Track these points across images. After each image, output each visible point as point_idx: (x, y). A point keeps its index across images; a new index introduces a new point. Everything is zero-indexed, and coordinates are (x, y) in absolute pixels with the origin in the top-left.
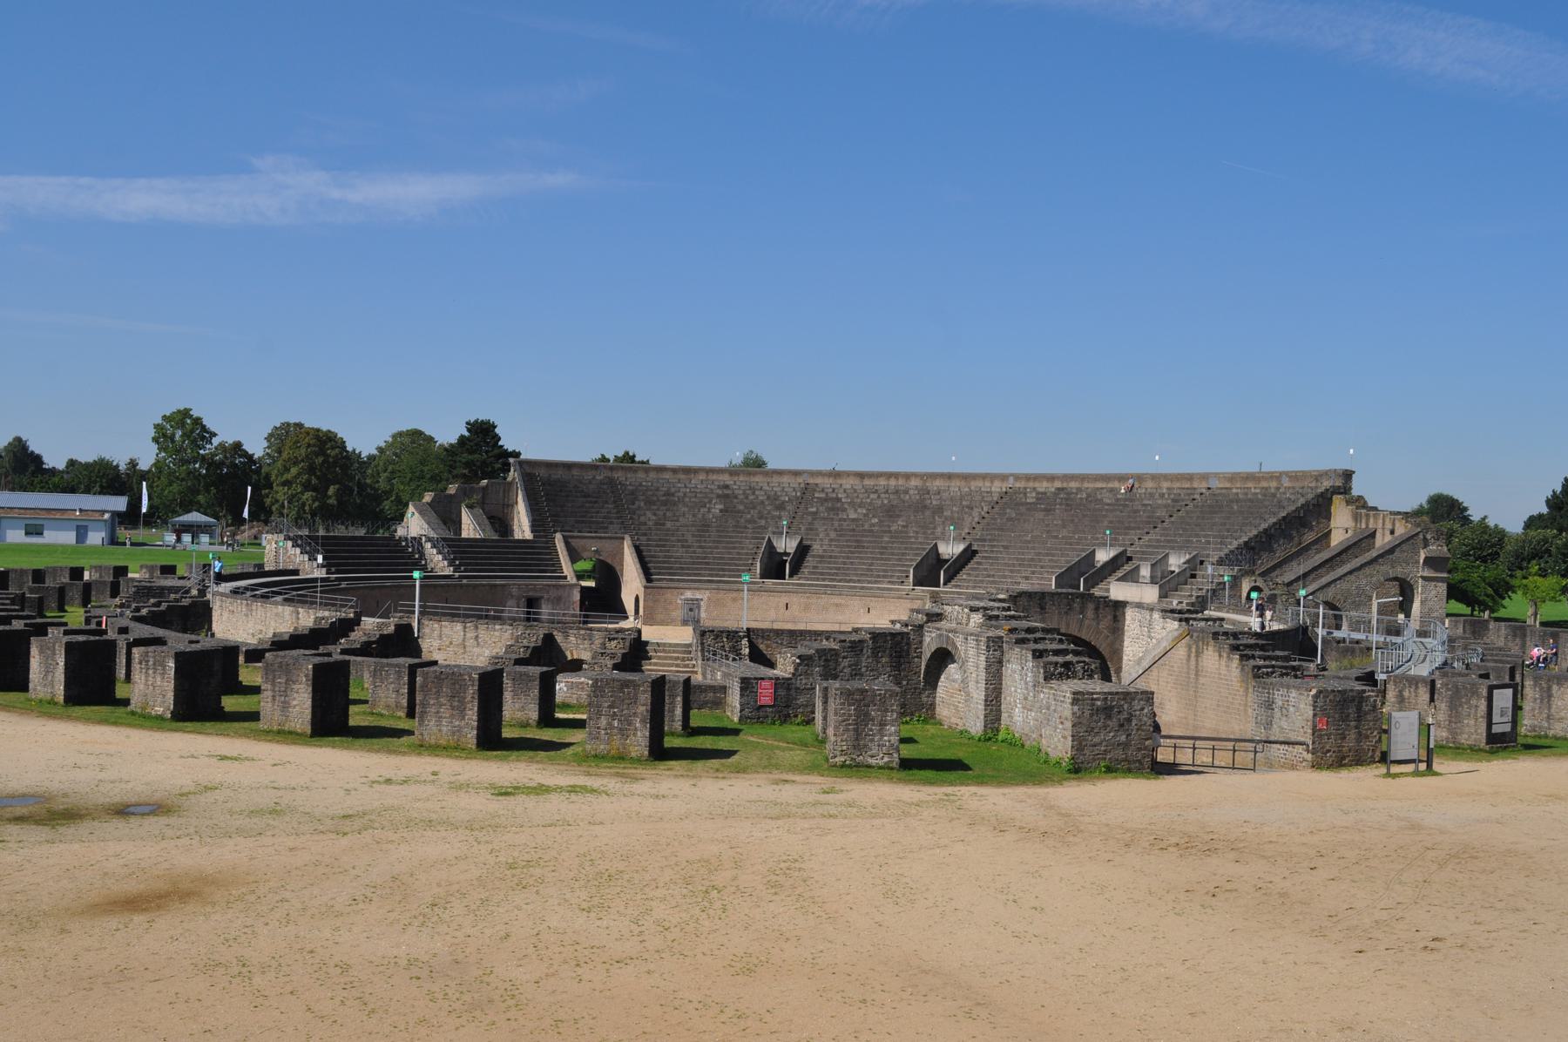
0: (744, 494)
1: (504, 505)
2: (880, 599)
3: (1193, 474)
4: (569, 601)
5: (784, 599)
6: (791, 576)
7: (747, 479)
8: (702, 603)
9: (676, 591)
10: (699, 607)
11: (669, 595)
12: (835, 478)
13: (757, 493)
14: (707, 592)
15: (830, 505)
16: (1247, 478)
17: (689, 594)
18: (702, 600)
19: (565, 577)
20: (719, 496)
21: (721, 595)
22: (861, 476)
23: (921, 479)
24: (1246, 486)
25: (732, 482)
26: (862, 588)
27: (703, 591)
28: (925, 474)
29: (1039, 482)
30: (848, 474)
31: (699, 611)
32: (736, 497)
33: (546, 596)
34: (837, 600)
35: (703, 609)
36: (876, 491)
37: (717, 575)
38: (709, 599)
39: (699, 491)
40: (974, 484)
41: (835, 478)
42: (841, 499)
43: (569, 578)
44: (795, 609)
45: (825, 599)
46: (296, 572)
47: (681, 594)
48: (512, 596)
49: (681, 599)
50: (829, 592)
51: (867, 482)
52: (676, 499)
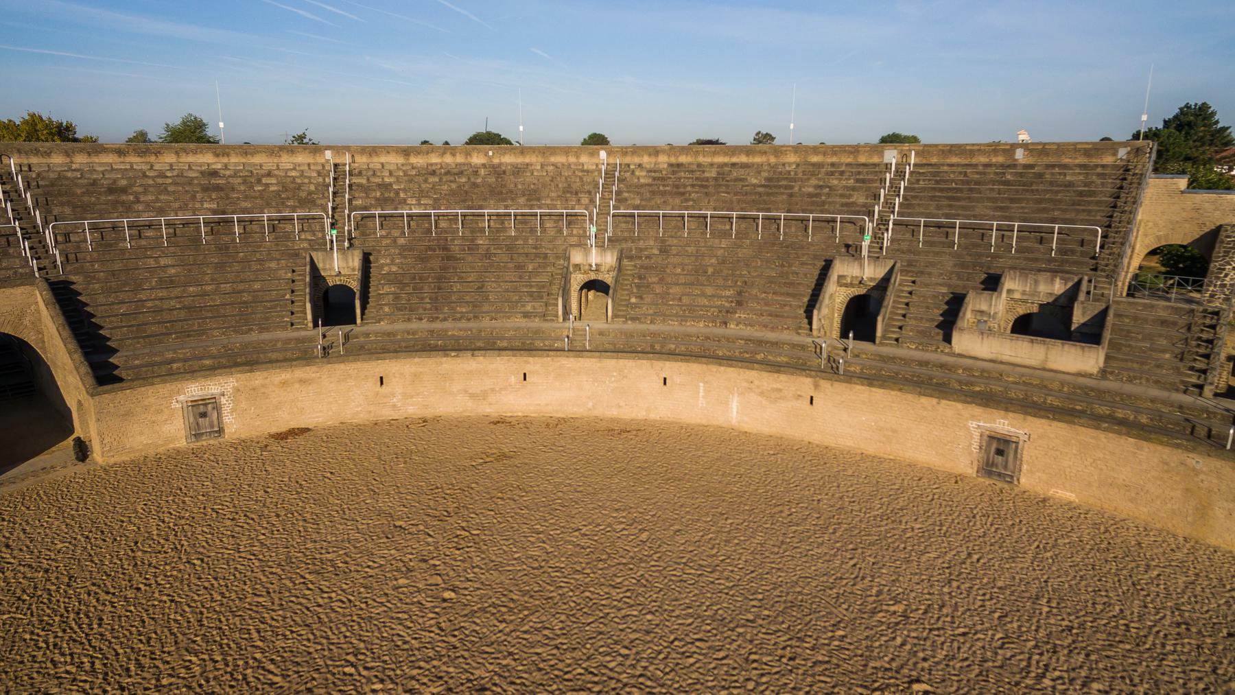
0: (245, 182)
3: (858, 146)
7: (244, 160)
8: (223, 400)
10: (218, 408)
13: (264, 180)
15: (378, 194)
16: (950, 151)
20: (205, 189)
24: (871, 161)
25: (219, 166)
30: (388, 150)
32: (233, 189)
35: (226, 411)
36: (433, 173)
39: (170, 181)
40: (560, 159)
42: (390, 184)
44: (395, 387)
47: (178, 393)
52: (131, 198)
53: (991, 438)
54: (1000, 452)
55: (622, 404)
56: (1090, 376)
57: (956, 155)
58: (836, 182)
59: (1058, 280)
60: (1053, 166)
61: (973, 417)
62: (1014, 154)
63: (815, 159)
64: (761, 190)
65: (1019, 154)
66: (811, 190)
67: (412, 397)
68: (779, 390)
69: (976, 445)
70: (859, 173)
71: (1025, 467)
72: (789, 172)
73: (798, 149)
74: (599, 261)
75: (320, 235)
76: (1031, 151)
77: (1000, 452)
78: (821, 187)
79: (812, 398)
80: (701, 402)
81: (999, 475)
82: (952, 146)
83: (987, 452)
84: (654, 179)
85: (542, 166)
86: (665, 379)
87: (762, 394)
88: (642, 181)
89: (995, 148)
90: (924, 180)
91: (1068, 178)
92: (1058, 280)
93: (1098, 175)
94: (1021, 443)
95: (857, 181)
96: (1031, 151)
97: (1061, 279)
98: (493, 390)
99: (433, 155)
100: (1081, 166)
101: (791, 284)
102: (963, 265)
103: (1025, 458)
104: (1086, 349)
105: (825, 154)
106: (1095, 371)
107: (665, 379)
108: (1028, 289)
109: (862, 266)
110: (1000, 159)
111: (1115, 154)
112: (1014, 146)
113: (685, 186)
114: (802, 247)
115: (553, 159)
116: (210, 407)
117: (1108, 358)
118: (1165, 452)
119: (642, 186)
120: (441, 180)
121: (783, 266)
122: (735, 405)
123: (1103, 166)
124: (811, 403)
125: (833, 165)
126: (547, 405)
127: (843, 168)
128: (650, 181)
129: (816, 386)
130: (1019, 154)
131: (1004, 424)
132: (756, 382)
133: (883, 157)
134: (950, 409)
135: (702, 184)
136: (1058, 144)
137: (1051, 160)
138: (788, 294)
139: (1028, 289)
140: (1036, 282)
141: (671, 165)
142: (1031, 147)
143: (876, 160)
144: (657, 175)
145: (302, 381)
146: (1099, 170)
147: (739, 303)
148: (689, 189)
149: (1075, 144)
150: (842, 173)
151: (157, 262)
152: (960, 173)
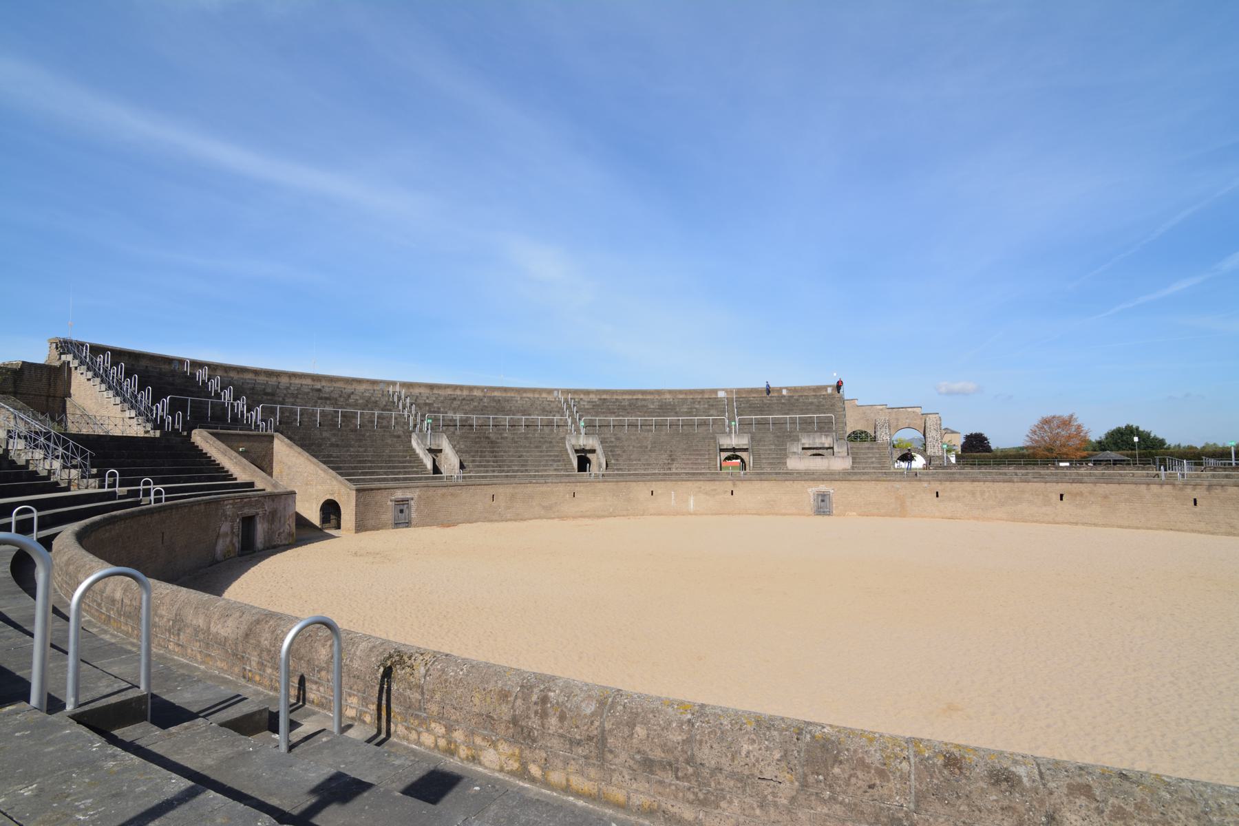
1: (48, 396)
2: (585, 484)
4: (285, 516)
5: (490, 490)
6: (442, 473)
8: (412, 503)
9: (385, 493)
10: (409, 508)
11: (379, 496)
12: (409, 388)
14: (418, 490)
17: (399, 495)
18: (412, 499)
19: (251, 485)
21: (430, 492)
22: (431, 387)
23: (482, 391)
26: (507, 476)
27: (413, 490)
28: (486, 388)
29: (577, 394)
31: (410, 512)
33: (260, 512)
34: (544, 488)
35: (413, 509)
37: (393, 473)
38: (419, 497)
41: (409, 388)
43: (259, 485)
45: (530, 489)
46: (264, 490)
48: (226, 516)
49: (391, 501)
50: (534, 481)
51: (435, 391)
53: (818, 495)
54: (823, 501)
55: (629, 508)
58: (697, 406)
59: (823, 436)
60: (802, 396)
61: (809, 487)
63: (681, 396)
64: (658, 410)
66: (686, 410)
67: (509, 509)
68: (715, 490)
69: (812, 500)
70: (708, 402)
71: (834, 505)
72: (670, 402)
73: (670, 392)
74: (585, 443)
75: (406, 428)
76: (790, 390)
77: (823, 501)
78: (691, 408)
79: (732, 491)
80: (673, 502)
81: (824, 512)
83: (818, 502)
84: (594, 406)
85: (521, 398)
86: (652, 492)
87: (706, 493)
88: (586, 407)
91: (810, 400)
92: (823, 436)
93: (823, 399)
94: (831, 495)
95: (709, 405)
96: (790, 390)
97: (825, 435)
98: (556, 503)
99: (448, 390)
100: (813, 395)
101: (697, 450)
102: (778, 437)
103: (834, 501)
105: (686, 394)
106: (849, 467)
107: (652, 492)
109: (731, 438)
111: (826, 391)
113: (614, 409)
114: (694, 434)
115: (524, 395)
116: (406, 506)
117: (853, 458)
118: (886, 484)
119: (588, 409)
120: (461, 403)
121: (687, 443)
122: (692, 502)
123: (824, 395)
124: (732, 494)
125: (693, 399)
126: (586, 511)
127: (699, 400)
128: (591, 407)
129: (734, 485)
130: (784, 392)
131: (823, 487)
132: (703, 487)
133: (717, 395)
134: (798, 485)
135: (624, 408)
136: (801, 387)
137: (800, 394)
138: (698, 454)
141: (600, 399)
143: (714, 396)
144: (594, 404)
145: (452, 494)
146: (822, 397)
147: (673, 460)
148: (616, 410)
149: (809, 387)
150: (699, 402)
151: (321, 434)
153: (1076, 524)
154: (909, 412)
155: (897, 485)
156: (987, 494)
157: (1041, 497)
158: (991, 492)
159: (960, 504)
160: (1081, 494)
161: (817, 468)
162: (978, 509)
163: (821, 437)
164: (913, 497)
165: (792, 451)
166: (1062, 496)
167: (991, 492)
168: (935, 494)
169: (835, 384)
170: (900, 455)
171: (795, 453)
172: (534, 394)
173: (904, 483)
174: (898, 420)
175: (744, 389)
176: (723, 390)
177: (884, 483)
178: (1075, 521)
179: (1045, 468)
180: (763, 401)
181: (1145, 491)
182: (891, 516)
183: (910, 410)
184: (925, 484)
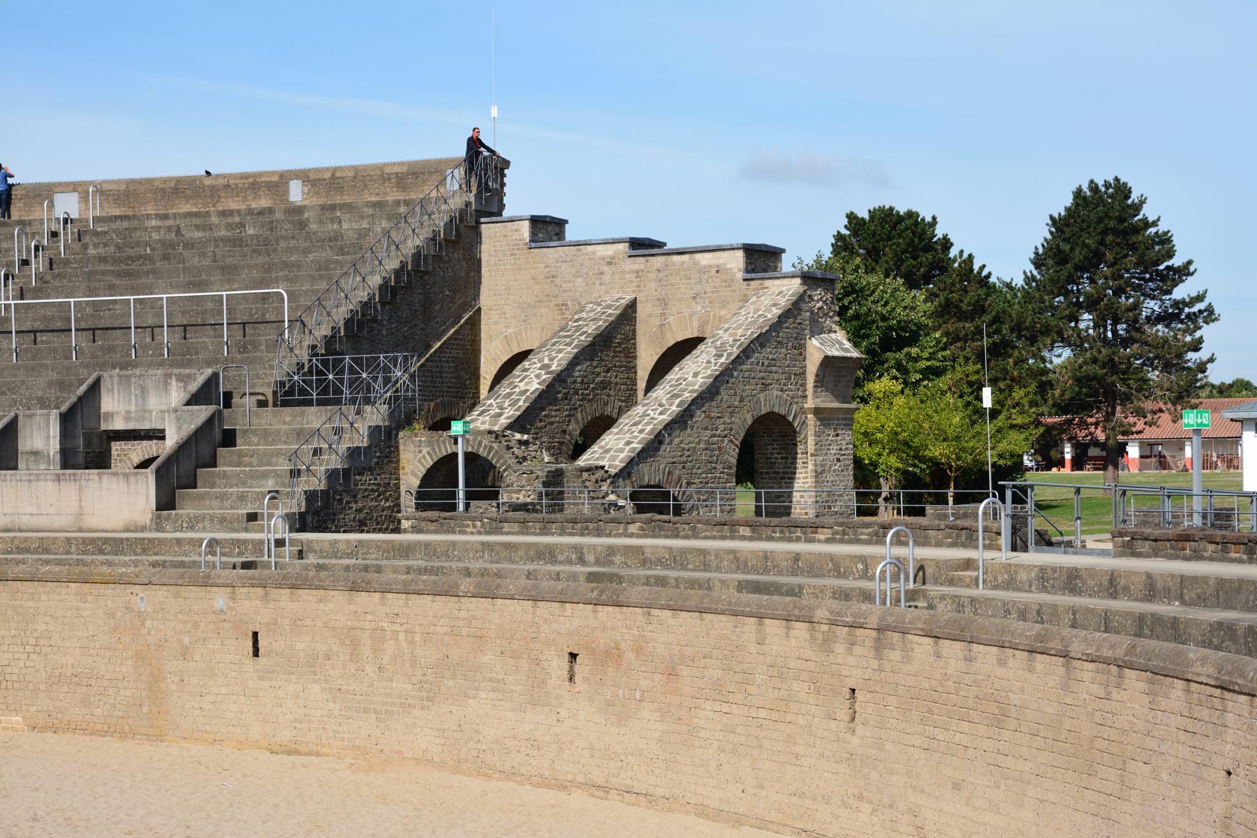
56: (143, 529)
57: (187, 199)
59: (174, 382)
62: (287, 191)
65: (296, 192)
82: (179, 180)
89: (253, 183)
90: (96, 246)
92: (174, 382)
104: (132, 479)
108: (133, 408)
110: (264, 203)
112: (285, 178)
130: (296, 192)
136: (356, 169)
139: (133, 408)
140: (143, 390)
142: (312, 177)
149: (381, 167)
152: (169, 228)
153: (604, 790)
154: (704, 270)
155: (143, 599)
156: (390, 645)
157: (524, 664)
158: (402, 636)
159: (316, 688)
160: (610, 656)
161: (43, 522)
162: (366, 711)
163: (166, 384)
164: (185, 654)
165: (28, 448)
166: (573, 656)
167: (402, 636)
168: (249, 643)
169: (461, 151)
170: (429, 463)
171: (35, 453)
172: (245, 198)
173: (160, 593)
174: (664, 303)
175: (150, 181)
176: (74, 187)
177: (107, 590)
178: (600, 781)
179: (766, 532)
180: (178, 231)
181: (753, 648)
182: (123, 736)
183: (705, 259)
184: (220, 599)
